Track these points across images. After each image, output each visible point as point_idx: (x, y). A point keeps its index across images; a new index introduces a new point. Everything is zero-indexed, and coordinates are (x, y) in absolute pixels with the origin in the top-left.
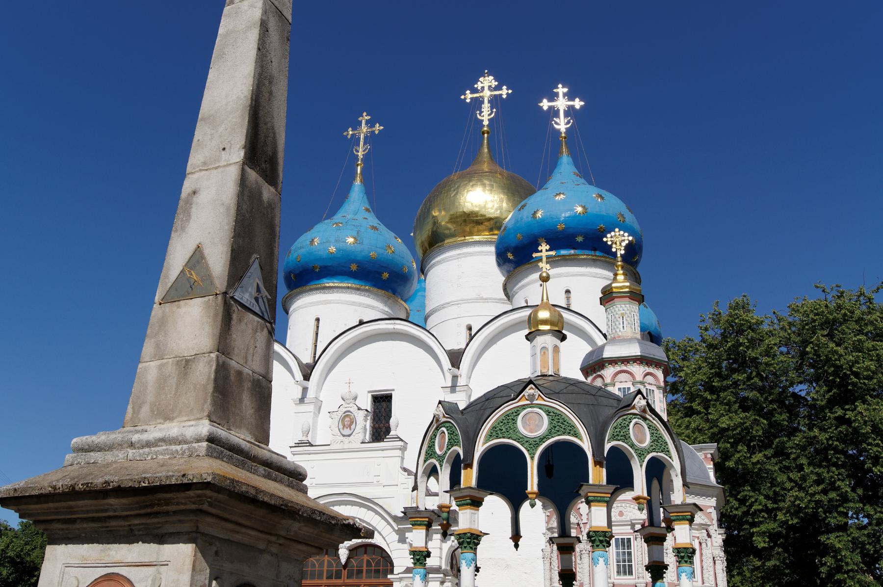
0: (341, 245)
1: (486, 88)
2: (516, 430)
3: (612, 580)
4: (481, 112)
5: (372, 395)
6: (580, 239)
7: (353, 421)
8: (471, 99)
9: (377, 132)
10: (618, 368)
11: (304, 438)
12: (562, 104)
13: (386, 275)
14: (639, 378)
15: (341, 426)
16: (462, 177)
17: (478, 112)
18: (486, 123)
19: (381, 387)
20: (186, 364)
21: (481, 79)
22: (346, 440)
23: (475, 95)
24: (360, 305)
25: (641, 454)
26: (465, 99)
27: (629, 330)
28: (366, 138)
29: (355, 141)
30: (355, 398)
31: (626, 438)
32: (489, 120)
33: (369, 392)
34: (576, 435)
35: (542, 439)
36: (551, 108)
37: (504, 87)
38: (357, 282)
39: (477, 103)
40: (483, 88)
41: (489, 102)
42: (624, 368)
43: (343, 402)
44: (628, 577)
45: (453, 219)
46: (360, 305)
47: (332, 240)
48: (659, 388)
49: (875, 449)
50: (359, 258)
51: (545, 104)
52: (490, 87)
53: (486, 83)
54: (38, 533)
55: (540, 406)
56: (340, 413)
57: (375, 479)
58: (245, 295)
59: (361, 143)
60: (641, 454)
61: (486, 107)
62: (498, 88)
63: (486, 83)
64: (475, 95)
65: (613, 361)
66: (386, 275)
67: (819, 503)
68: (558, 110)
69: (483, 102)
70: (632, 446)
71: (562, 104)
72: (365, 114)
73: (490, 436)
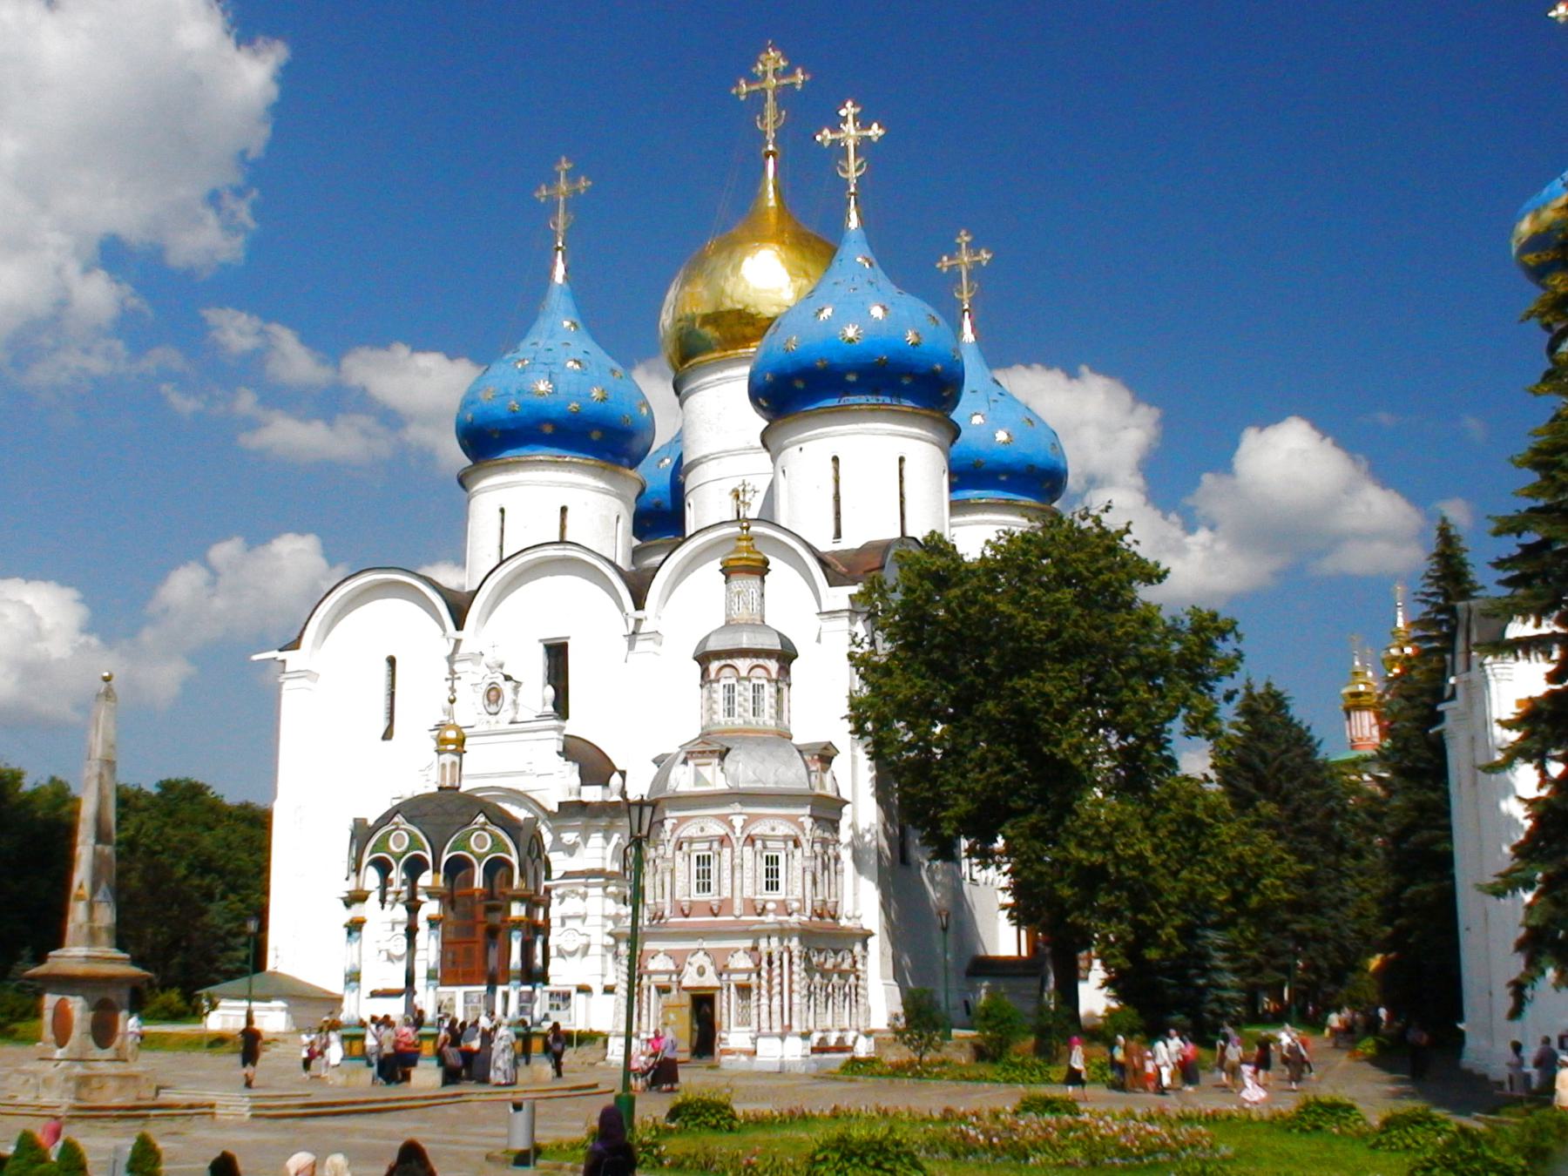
0: (527, 397)
1: (770, 75)
2: (388, 847)
3: (693, 898)
4: (763, 118)
5: (546, 646)
6: (852, 378)
7: (499, 694)
8: (747, 93)
9: (582, 191)
10: (723, 662)
11: (446, 718)
12: (850, 132)
13: (595, 435)
14: (744, 673)
15: (486, 702)
16: (718, 251)
17: (758, 118)
18: (771, 136)
19: (555, 633)
20: (81, 926)
21: (763, 57)
22: (493, 719)
23: (755, 87)
24: (561, 484)
25: (480, 858)
26: (738, 94)
27: (745, 611)
28: (566, 200)
29: (552, 205)
30: (501, 666)
31: (466, 847)
32: (775, 131)
33: (541, 641)
34: (425, 851)
35: (404, 853)
36: (835, 143)
37: (799, 71)
38: (555, 451)
39: (758, 99)
40: (765, 73)
41: (775, 99)
42: (729, 662)
43: (488, 671)
44: (706, 894)
45: (715, 319)
46: (561, 484)
47: (513, 391)
48: (769, 681)
49: (1046, 726)
50: (554, 415)
51: (825, 136)
52: (775, 70)
53: (772, 60)
54: (184, 799)
55: (405, 830)
56: (485, 687)
57: (527, 768)
58: (99, 897)
59: (561, 211)
60: (480, 858)
61: (770, 103)
62: (789, 72)
63: (772, 60)
64: (755, 87)
65: (718, 655)
66: (595, 435)
67: (997, 785)
68: (846, 147)
69: (766, 101)
70: (472, 853)
71: (850, 132)
72: (564, 159)
73: (372, 853)
